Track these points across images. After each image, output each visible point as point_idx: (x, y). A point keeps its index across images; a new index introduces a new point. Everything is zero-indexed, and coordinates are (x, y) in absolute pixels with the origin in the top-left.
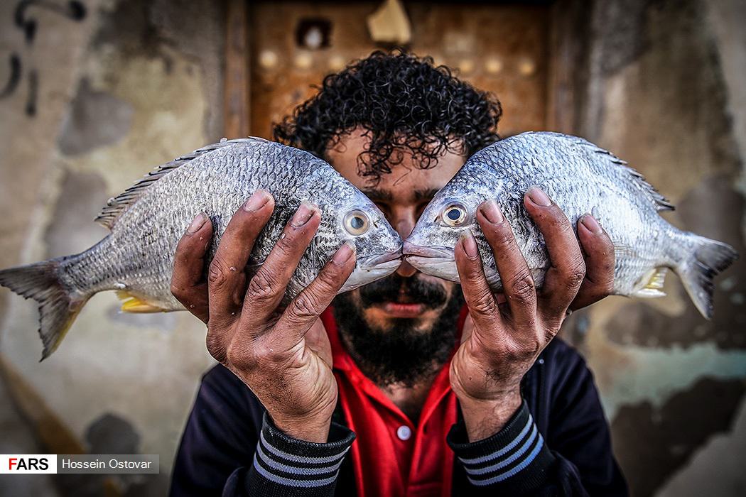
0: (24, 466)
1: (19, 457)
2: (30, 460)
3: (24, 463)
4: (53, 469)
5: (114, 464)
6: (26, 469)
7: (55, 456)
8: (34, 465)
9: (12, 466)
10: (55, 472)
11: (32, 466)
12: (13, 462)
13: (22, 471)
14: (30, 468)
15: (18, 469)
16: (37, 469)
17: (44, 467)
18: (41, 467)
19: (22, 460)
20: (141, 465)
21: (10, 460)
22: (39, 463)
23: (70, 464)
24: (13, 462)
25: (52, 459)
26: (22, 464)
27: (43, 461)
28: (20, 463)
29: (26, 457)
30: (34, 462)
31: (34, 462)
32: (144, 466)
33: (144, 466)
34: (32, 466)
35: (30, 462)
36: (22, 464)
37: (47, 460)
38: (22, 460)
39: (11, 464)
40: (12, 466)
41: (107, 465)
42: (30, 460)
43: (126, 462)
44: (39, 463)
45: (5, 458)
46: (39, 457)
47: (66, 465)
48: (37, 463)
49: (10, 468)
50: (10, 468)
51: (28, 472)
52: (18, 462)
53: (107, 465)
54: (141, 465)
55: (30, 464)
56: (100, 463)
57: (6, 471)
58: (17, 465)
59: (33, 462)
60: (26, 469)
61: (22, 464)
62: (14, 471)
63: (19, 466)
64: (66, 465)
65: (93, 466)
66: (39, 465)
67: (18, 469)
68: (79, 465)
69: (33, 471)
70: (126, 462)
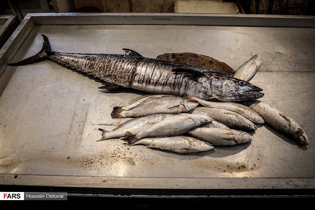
0: (10, 197)
1: (8, 193)
2: (13, 194)
3: (10, 196)
4: (22, 198)
5: (48, 196)
6: (11, 198)
7: (23, 193)
8: (14, 196)
9: (5, 197)
10: (23, 199)
11: (14, 197)
12: (5, 195)
13: (9, 199)
14: (13, 198)
15: (8, 198)
16: (16, 198)
17: (19, 197)
18: (17, 198)
19: (9, 194)
20: (59, 196)
21: (4, 194)
22: (16, 195)
23: (29, 196)
24: (5, 195)
25: (22, 194)
26: (9, 196)
27: (18, 195)
28: (9, 196)
29: (11, 193)
30: (14, 195)
31: (14, 195)
32: (61, 197)
33: (61, 197)
34: (14, 197)
35: (13, 195)
36: (9, 196)
37: (20, 195)
38: (9, 194)
39: (5, 196)
40: (5, 197)
41: (45, 196)
42: (13, 194)
43: (53, 195)
44: (16, 195)
45: (2, 194)
46: (16, 193)
47: (28, 197)
48: (15, 196)
49: (4, 198)
50: (4, 198)
51: (12, 199)
52: (7, 195)
53: (45, 196)
54: (59, 196)
55: (13, 196)
56: (42, 196)
57: (3, 199)
58: (7, 196)
59: (14, 195)
60: (11, 198)
61: (9, 196)
62: (6, 199)
63: (8, 197)
64: (28, 197)
65: (39, 197)
66: (16, 196)
67: (8, 198)
68: (33, 197)
69: (14, 199)
70: (53, 195)
